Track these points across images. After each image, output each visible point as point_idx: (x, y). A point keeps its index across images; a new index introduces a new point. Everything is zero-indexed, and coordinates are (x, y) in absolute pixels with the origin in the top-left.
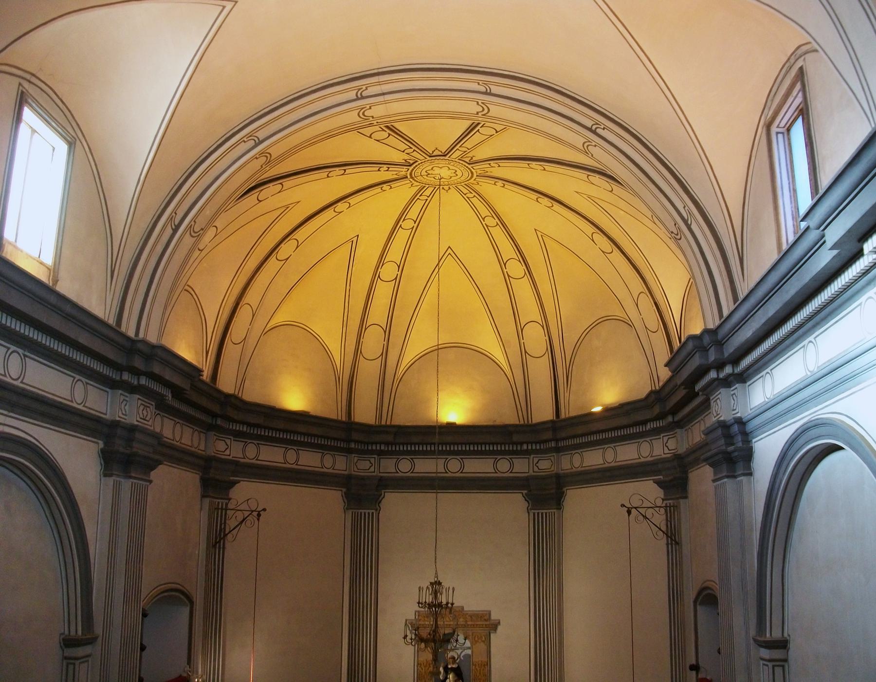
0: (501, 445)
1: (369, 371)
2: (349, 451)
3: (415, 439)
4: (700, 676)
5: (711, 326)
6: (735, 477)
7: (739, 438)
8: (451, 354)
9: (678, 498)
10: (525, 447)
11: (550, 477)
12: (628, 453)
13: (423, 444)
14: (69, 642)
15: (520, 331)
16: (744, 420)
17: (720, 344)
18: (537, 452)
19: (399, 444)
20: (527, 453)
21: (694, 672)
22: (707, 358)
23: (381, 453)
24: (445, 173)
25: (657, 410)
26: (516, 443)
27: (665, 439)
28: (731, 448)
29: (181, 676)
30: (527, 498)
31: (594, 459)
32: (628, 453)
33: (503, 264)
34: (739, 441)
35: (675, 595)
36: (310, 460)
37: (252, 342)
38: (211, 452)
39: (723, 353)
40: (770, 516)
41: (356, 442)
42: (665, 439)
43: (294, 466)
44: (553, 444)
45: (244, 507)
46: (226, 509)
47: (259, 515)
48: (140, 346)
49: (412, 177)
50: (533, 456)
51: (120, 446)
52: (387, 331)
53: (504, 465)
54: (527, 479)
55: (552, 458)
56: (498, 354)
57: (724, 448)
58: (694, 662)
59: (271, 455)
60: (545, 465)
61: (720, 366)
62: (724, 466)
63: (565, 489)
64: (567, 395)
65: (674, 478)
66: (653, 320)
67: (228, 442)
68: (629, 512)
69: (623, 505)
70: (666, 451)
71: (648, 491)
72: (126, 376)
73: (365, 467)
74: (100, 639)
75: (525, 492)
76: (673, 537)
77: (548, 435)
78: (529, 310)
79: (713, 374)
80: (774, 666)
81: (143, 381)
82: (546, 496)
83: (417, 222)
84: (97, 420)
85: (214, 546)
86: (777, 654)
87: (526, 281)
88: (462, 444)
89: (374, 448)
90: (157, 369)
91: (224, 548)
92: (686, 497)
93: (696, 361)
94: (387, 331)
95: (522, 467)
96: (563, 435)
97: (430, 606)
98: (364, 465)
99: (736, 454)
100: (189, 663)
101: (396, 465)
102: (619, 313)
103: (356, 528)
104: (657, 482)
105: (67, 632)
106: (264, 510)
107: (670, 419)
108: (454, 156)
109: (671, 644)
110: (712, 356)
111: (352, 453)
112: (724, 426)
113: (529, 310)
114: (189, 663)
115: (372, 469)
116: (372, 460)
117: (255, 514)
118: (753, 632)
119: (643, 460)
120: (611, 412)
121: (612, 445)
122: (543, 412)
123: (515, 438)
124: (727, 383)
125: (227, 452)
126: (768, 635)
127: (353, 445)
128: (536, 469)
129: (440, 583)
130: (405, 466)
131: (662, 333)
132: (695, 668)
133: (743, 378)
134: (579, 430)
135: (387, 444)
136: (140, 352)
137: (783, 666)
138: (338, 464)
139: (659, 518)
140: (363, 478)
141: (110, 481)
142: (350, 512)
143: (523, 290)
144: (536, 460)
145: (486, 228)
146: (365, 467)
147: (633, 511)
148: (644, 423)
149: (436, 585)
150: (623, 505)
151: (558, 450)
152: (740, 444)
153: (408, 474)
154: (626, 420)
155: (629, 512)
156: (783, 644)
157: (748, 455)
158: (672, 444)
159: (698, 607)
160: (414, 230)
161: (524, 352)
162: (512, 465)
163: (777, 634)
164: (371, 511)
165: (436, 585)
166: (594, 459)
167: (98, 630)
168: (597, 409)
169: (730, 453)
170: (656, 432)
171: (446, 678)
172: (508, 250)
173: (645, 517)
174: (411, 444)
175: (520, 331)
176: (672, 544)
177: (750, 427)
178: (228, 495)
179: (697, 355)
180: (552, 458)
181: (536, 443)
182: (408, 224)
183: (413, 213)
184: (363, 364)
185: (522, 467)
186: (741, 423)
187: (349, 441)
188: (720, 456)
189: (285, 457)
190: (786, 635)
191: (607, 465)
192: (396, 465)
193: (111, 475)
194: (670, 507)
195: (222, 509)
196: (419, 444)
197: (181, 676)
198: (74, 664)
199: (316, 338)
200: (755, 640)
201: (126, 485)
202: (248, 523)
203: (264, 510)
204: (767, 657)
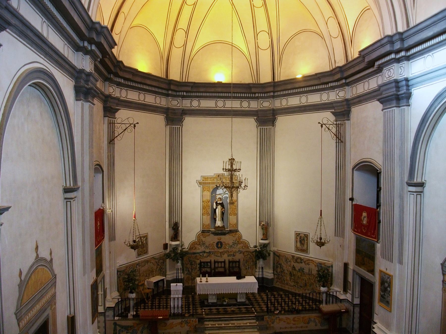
0: (249, 94)
1: (177, 54)
2: (167, 95)
3: (202, 90)
4: (354, 203)
5: (400, 30)
6: (399, 107)
7: (405, 88)
8: (219, 46)
9: (344, 120)
10: (257, 95)
11: (270, 110)
12: (314, 98)
13: (205, 92)
14: (67, 190)
16: (409, 79)
17: (402, 40)
18: (262, 98)
19: (193, 92)
20: (258, 98)
21: (351, 201)
22: (393, 47)
23: (183, 97)
25: (338, 76)
26: (252, 93)
27: (338, 92)
28: (399, 93)
29: (100, 209)
30: (257, 120)
31: (294, 101)
32: (314, 98)
34: (403, 90)
35: (340, 167)
36: (150, 99)
37: (123, 33)
38: (107, 93)
39: (403, 45)
40: (424, 124)
41: (172, 90)
42: (338, 92)
43: (143, 102)
44: (272, 94)
45: (126, 122)
46: (114, 123)
47: (135, 126)
48: (97, 26)
50: (262, 100)
51: (82, 83)
52: (187, 33)
53: (245, 104)
54: (257, 111)
55: (270, 101)
56: (244, 48)
57: (395, 92)
58: (351, 197)
59: (133, 96)
60: (266, 104)
61: (398, 52)
62: (395, 101)
63: (277, 116)
64: (279, 69)
65: (343, 111)
66: (335, 31)
67: (114, 87)
68: (322, 126)
69: (319, 123)
70: (338, 97)
71: (327, 116)
72: (86, 44)
73: (175, 103)
74: (80, 188)
75: (255, 118)
76: (340, 139)
77: (271, 89)
78: (262, 24)
79: (393, 56)
80: (417, 195)
81: (94, 47)
82: (267, 119)
84: (73, 67)
85: (110, 143)
86: (419, 189)
87: (262, 10)
88: (225, 93)
89: (180, 94)
90: (103, 41)
91: (114, 144)
92: (349, 120)
93: (388, 48)
94: (187, 33)
95: (254, 105)
96: (279, 89)
97: (229, 170)
98: (175, 103)
99: (404, 95)
100: (103, 202)
101: (191, 103)
102: (313, 28)
103: (171, 135)
104: (333, 113)
105: (65, 185)
106: (138, 123)
107: (344, 81)
109: (336, 189)
110: (397, 46)
111: (169, 96)
112: (397, 82)
113: (262, 24)
114: (103, 202)
115: (179, 105)
116: (179, 100)
117: (132, 125)
118: (406, 179)
119: (323, 102)
120: (307, 78)
121: (305, 95)
122: (266, 77)
123: (253, 90)
124: (398, 61)
125: (114, 94)
126: (415, 180)
127: (170, 92)
128: (262, 106)
129: (234, 159)
130: (195, 103)
131: (340, 39)
132: (352, 199)
133: (408, 58)
134: (289, 86)
135: (187, 92)
136: (96, 29)
137: (421, 195)
138: (162, 102)
139: (334, 130)
140: (174, 110)
141: (80, 103)
142: (168, 126)
143: (260, 13)
144: (262, 102)
146: (175, 103)
147: (324, 125)
148: (327, 83)
149: (232, 161)
150: (319, 123)
151: (273, 97)
152: (405, 91)
153: (197, 108)
154: (318, 81)
155: (322, 126)
156: (422, 185)
157: (408, 96)
158: (342, 94)
159: (355, 172)
161: (257, 47)
162: (249, 104)
163: (419, 180)
164: (178, 126)
165: (232, 161)
166: (294, 101)
167: (79, 184)
168: (299, 76)
169: (398, 95)
170: (333, 88)
171: (217, 208)
173: (329, 129)
174: (199, 92)
176: (339, 142)
177: (410, 83)
178: (115, 116)
179: (389, 45)
180: (270, 101)
181: (262, 93)
184: (174, 50)
185: (254, 105)
186: (407, 80)
187: (168, 90)
188: (394, 96)
189: (139, 97)
190: (423, 181)
191: (302, 104)
192: (191, 103)
193: (80, 100)
194: (339, 124)
195: (112, 123)
196: (203, 92)
197: (100, 209)
198: (70, 201)
199: (151, 34)
200: (407, 183)
201: (87, 105)
202: (129, 130)
203: (138, 123)
204: (414, 190)
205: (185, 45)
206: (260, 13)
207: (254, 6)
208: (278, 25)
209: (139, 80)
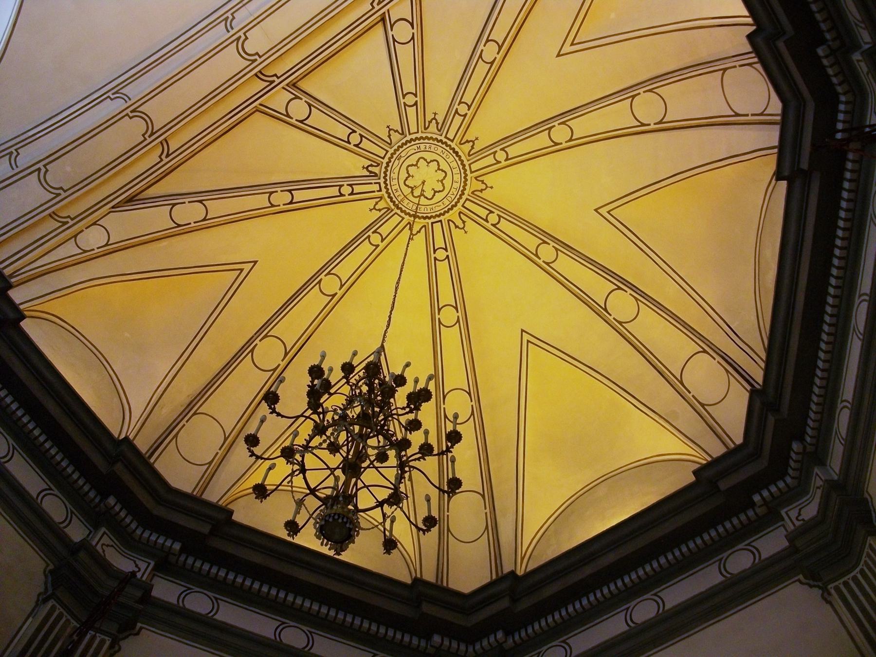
15: (677, 384)
24: (426, 175)
33: (602, 311)
49: (398, 208)
53: (740, 561)
78: (672, 345)
83: (459, 305)
87: (648, 315)
95: (772, 543)
108: (413, 129)
113: (672, 345)
143: (652, 328)
145: (548, 268)
160: (463, 322)
172: (597, 287)
175: (677, 384)
182: (448, 316)
183: (446, 296)
185: (772, 543)
205: (493, 527)
206: (652, 328)
207: (620, 323)
208: (700, 301)
209: (257, 558)
